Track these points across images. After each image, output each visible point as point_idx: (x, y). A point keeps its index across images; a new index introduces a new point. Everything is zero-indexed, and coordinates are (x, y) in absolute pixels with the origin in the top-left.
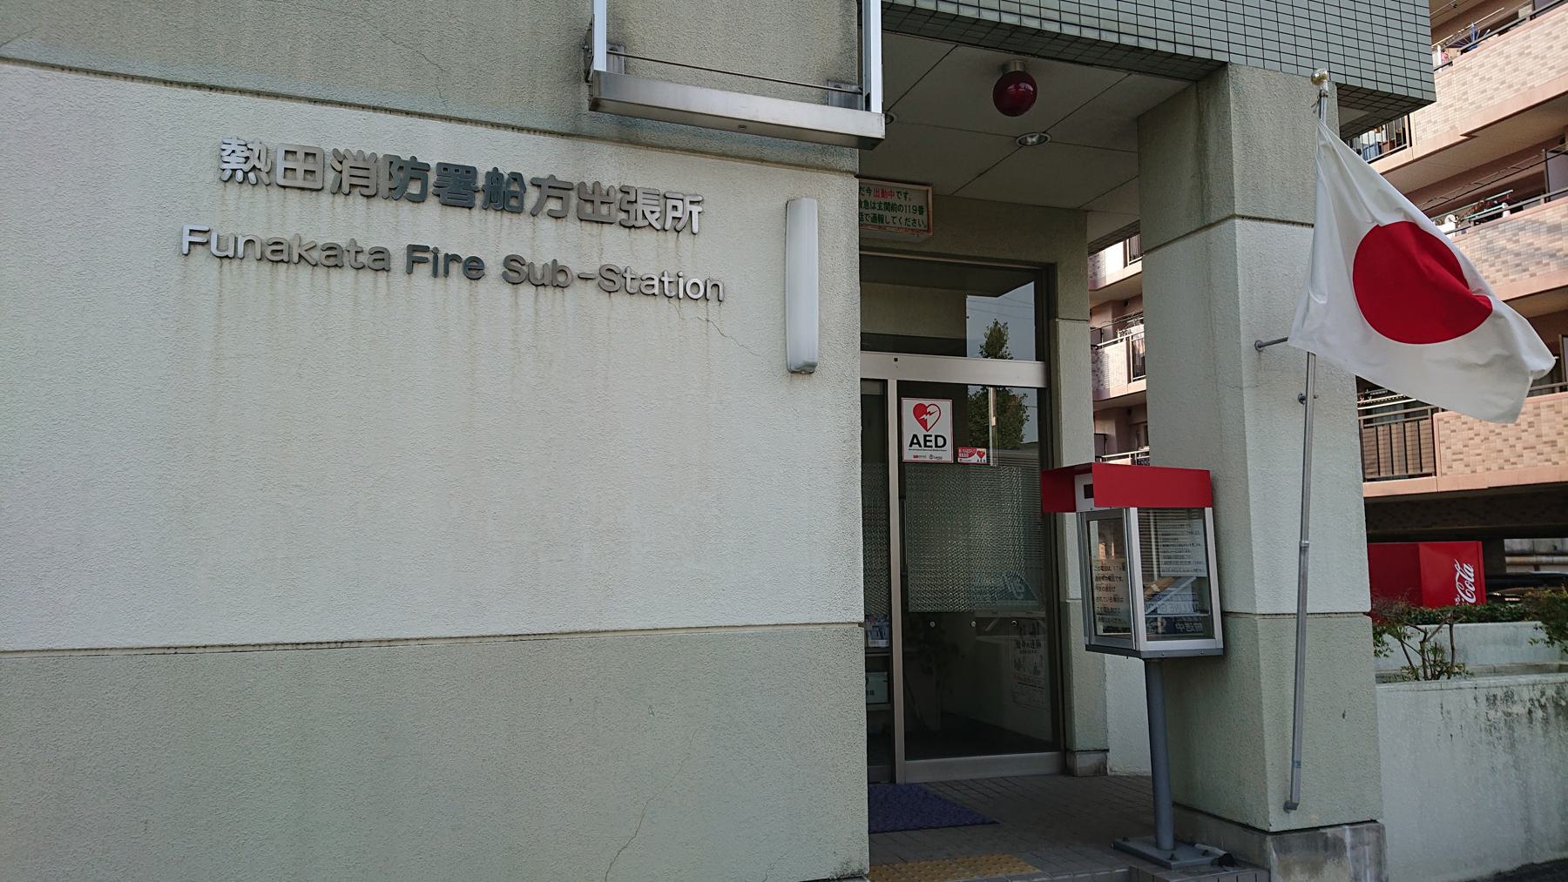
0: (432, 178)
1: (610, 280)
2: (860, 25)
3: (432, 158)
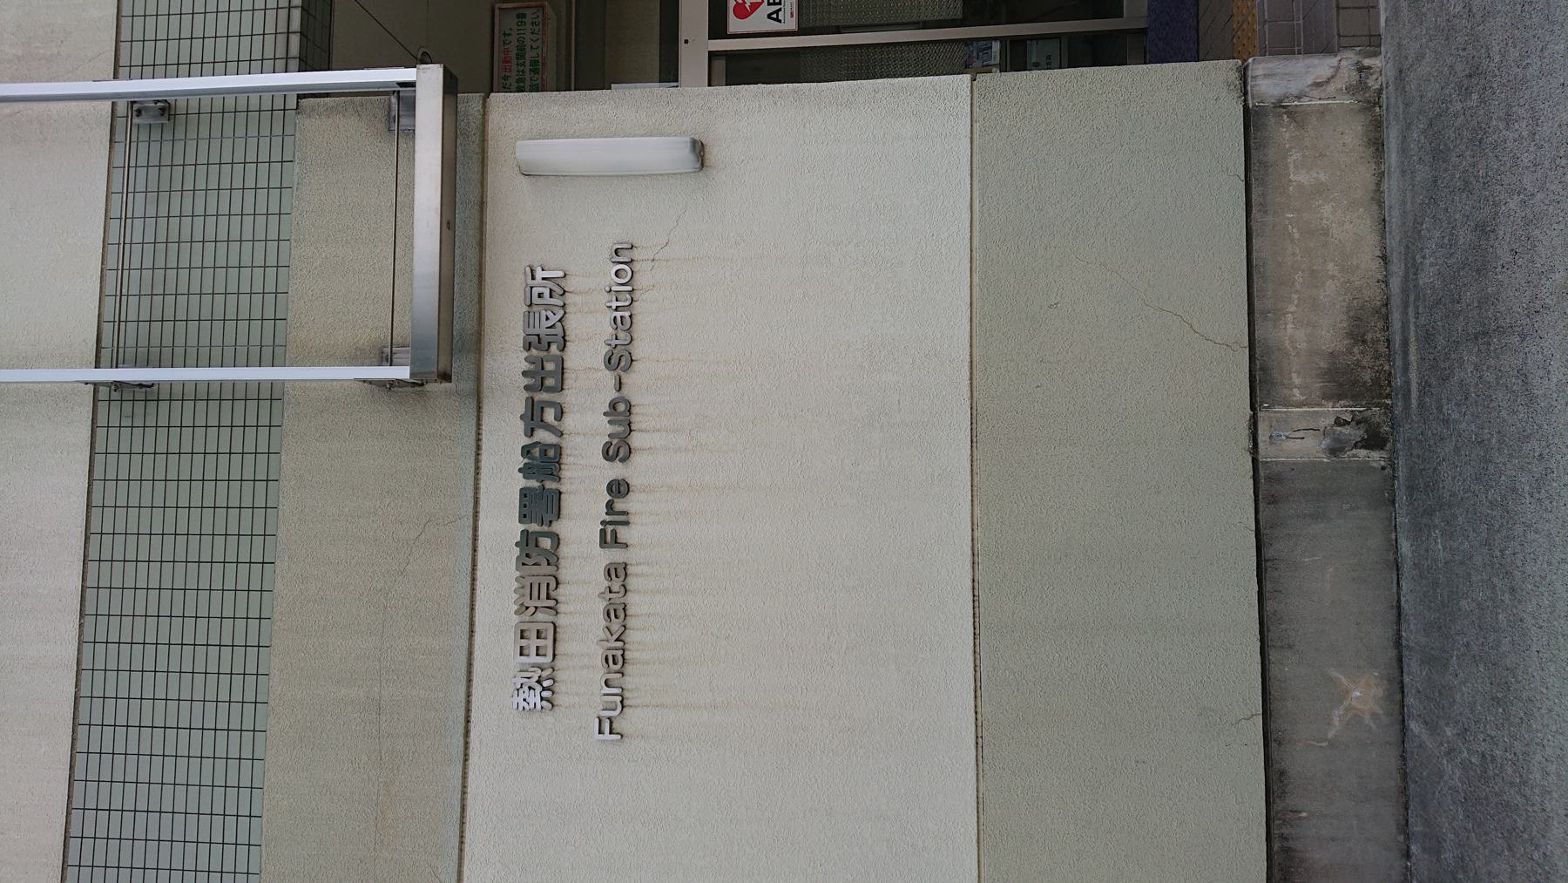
0: (534, 527)
1: (619, 360)
2: (327, 95)
3: (516, 529)
